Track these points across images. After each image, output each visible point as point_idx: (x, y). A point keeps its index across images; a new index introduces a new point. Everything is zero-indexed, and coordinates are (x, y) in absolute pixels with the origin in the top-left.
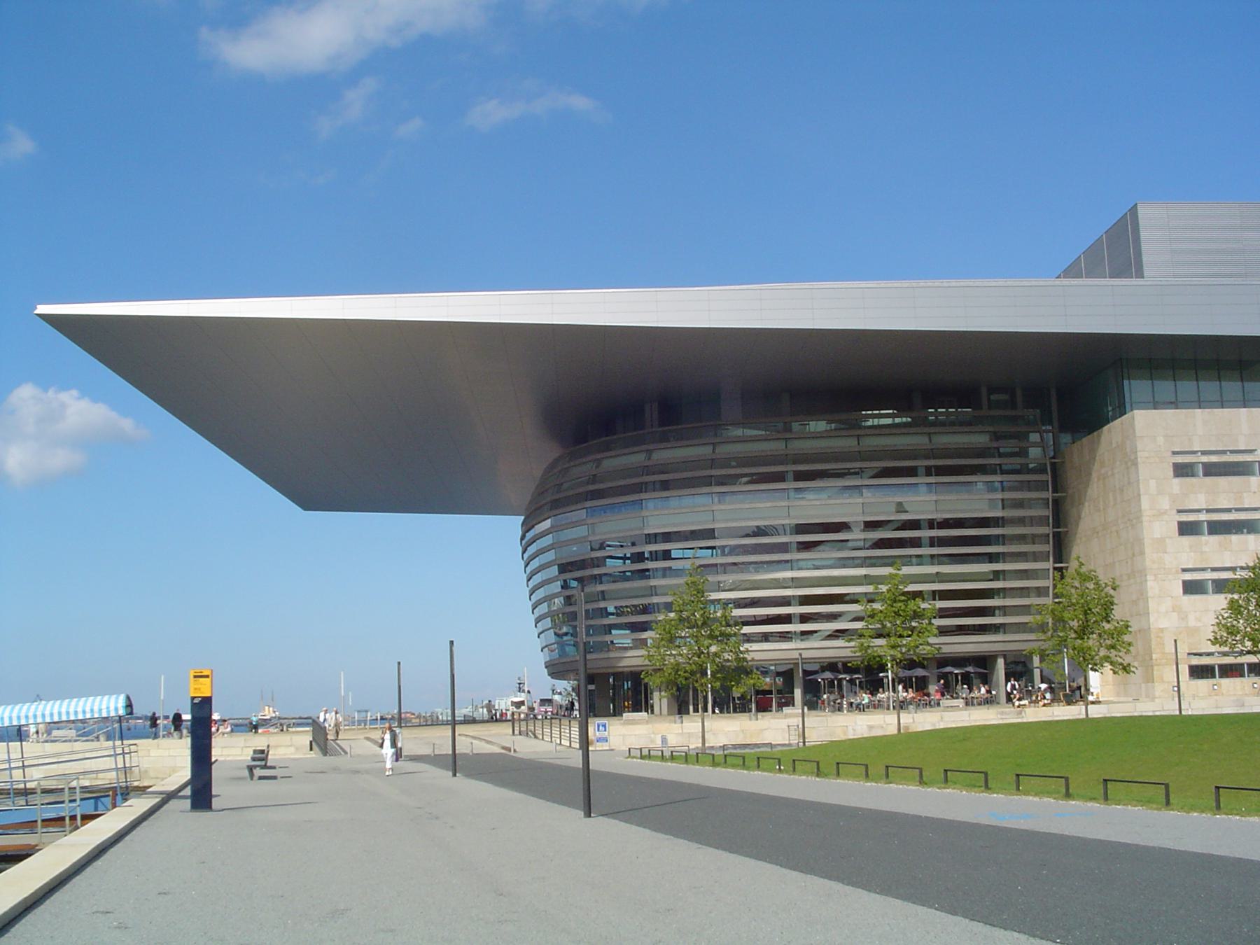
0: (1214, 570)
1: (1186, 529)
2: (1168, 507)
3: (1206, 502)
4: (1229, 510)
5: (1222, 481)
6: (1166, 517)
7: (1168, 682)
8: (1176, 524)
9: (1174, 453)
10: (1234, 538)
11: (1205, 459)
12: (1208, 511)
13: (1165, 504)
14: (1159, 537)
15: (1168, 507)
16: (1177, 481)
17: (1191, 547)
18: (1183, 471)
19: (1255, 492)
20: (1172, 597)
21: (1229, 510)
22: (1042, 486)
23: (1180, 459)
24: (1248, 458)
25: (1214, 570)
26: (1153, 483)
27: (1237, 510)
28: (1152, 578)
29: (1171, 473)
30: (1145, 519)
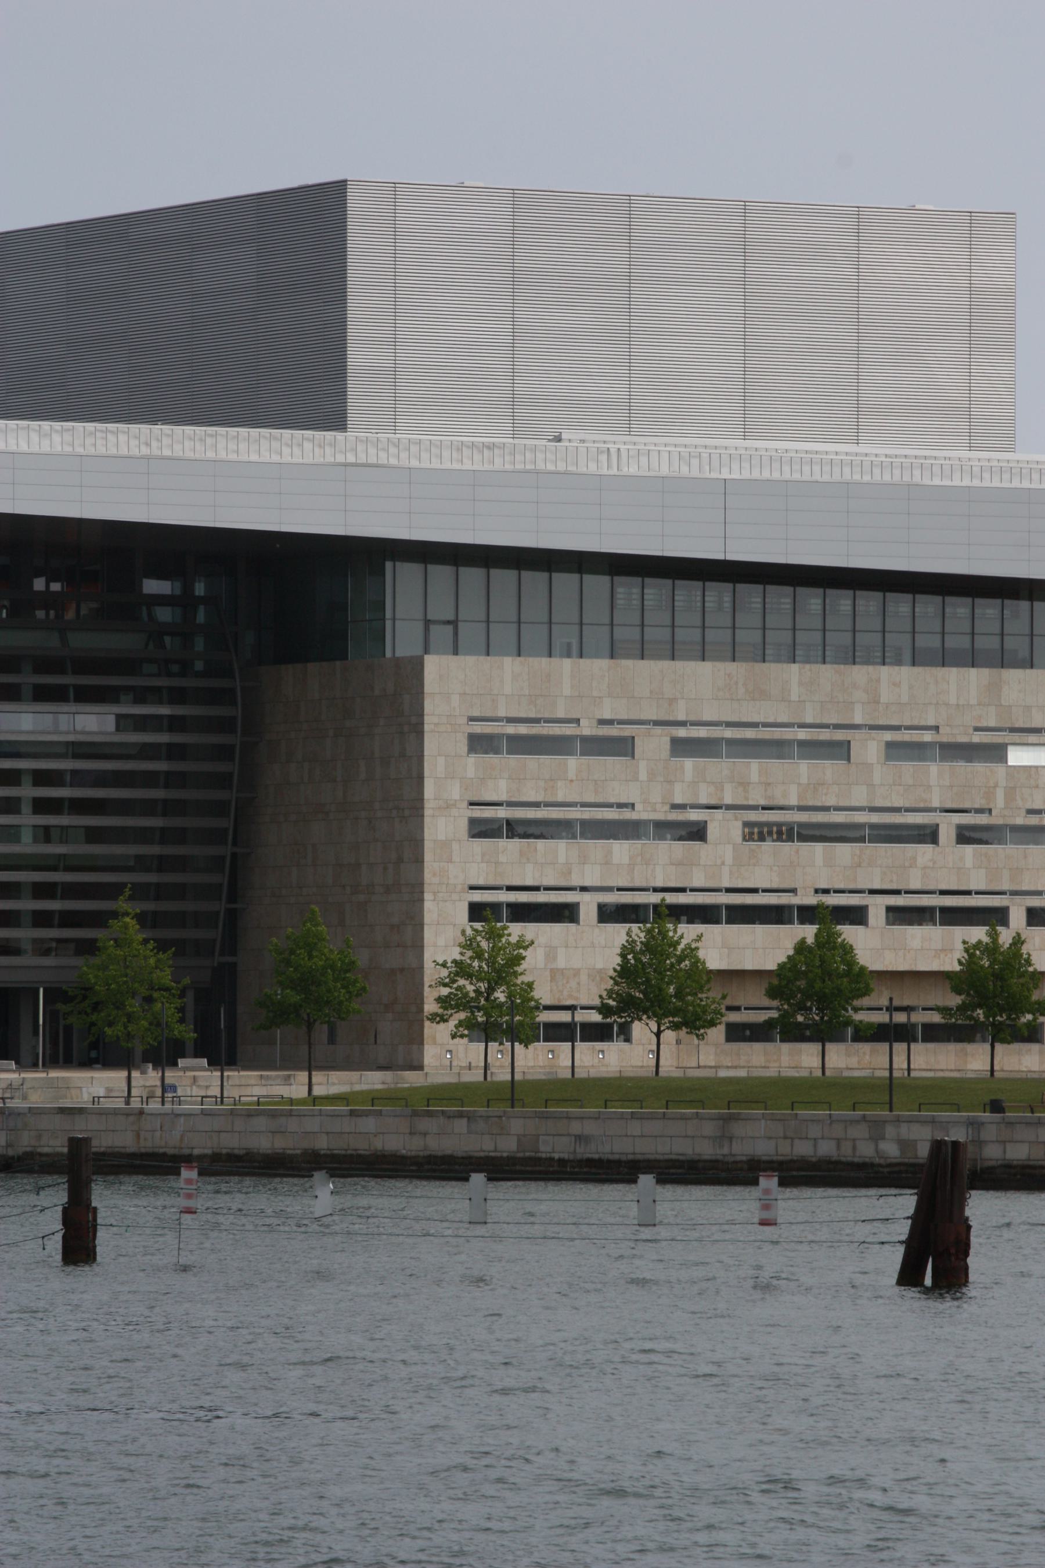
0: (510, 888)
1: (481, 830)
2: (457, 797)
3: (507, 792)
4: (536, 805)
5: (533, 762)
6: (454, 812)
7: (442, 1045)
8: (466, 822)
9: (472, 719)
10: (540, 844)
11: (511, 729)
12: (510, 804)
13: (455, 792)
14: (444, 839)
15: (457, 797)
16: (472, 760)
17: (483, 855)
18: (480, 744)
19: (572, 781)
20: (455, 925)
21: (536, 805)
22: (225, 725)
23: (478, 728)
24: (568, 730)
25: (510, 888)
26: (441, 760)
27: (548, 805)
28: (432, 898)
29: (465, 749)
30: (427, 812)
